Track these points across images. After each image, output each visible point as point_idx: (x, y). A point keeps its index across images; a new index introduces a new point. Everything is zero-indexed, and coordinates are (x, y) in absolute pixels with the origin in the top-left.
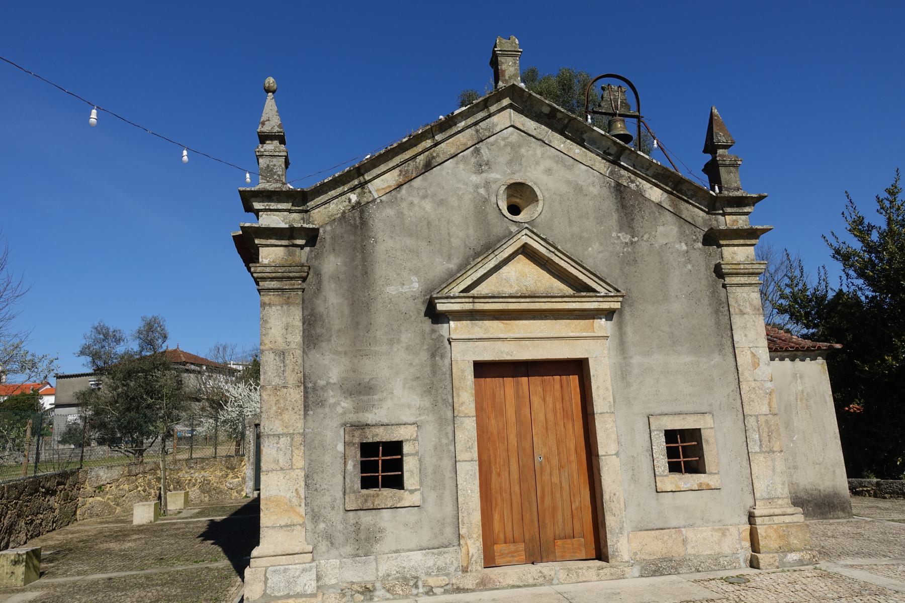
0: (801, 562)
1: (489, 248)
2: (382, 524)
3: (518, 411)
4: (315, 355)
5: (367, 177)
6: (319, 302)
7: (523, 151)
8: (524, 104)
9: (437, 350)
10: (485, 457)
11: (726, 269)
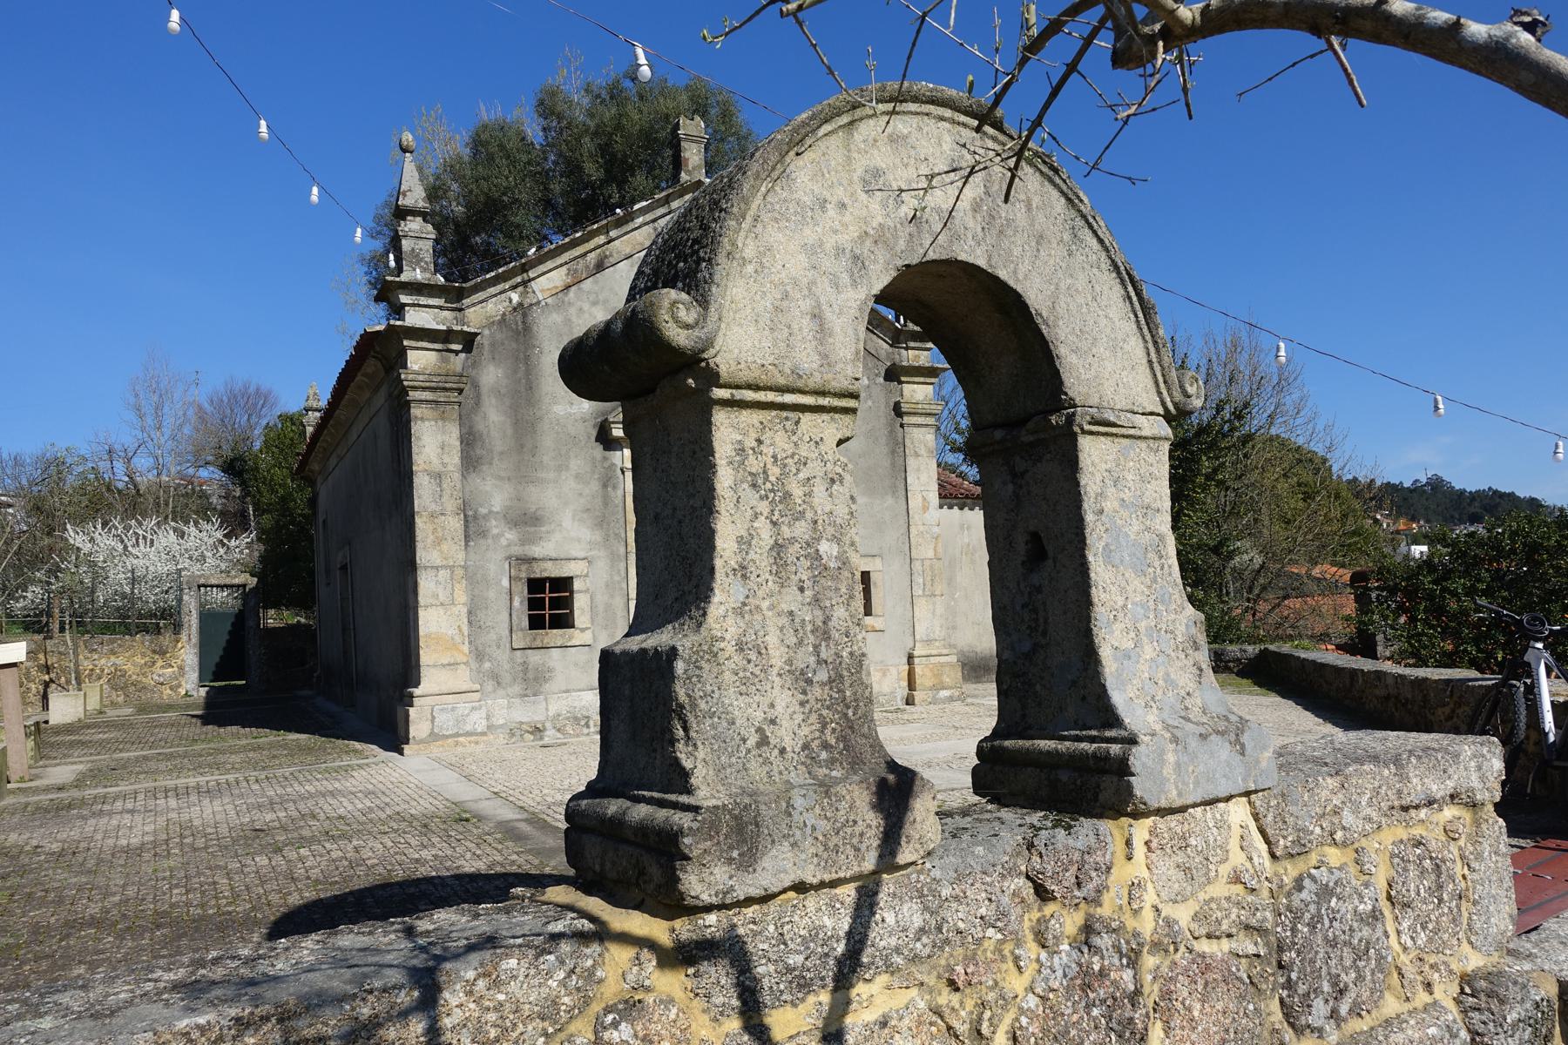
0: (951, 699)
2: (551, 664)
4: (474, 480)
5: (532, 274)
6: (477, 419)
11: (905, 408)
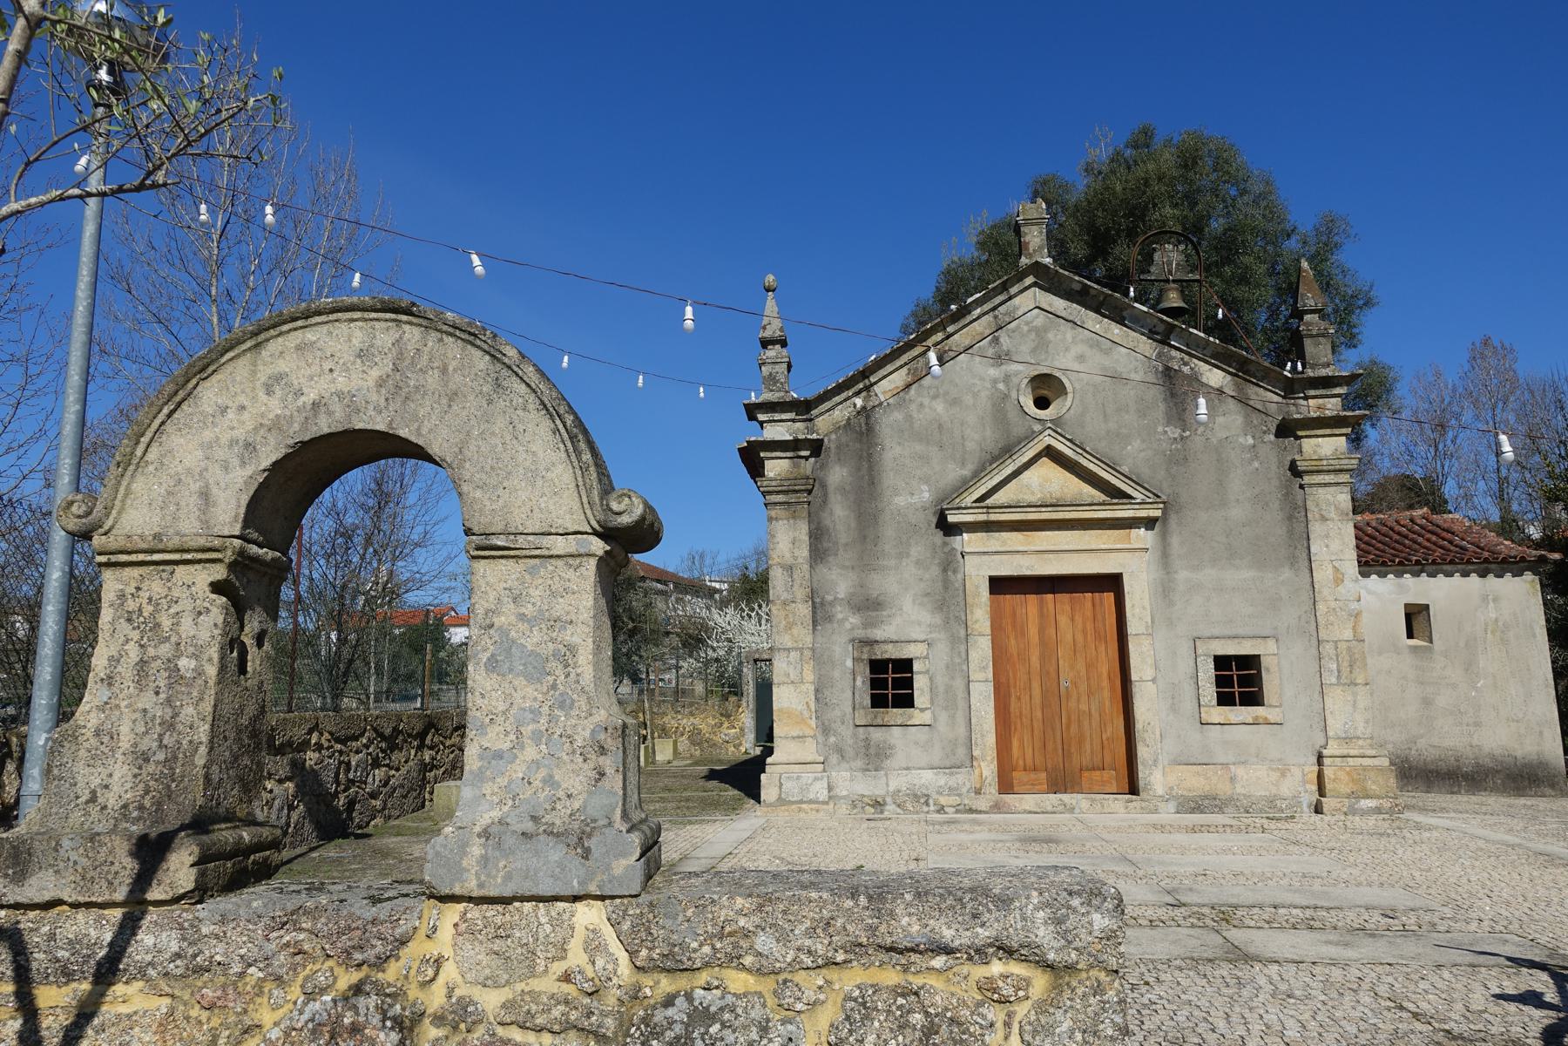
0: (1378, 810)
1: (1007, 451)
2: (893, 741)
3: (1042, 630)
4: (822, 569)
5: (873, 379)
6: (825, 515)
7: (1050, 336)
8: (1049, 282)
9: (950, 564)
10: (1003, 680)
11: (1301, 466)
